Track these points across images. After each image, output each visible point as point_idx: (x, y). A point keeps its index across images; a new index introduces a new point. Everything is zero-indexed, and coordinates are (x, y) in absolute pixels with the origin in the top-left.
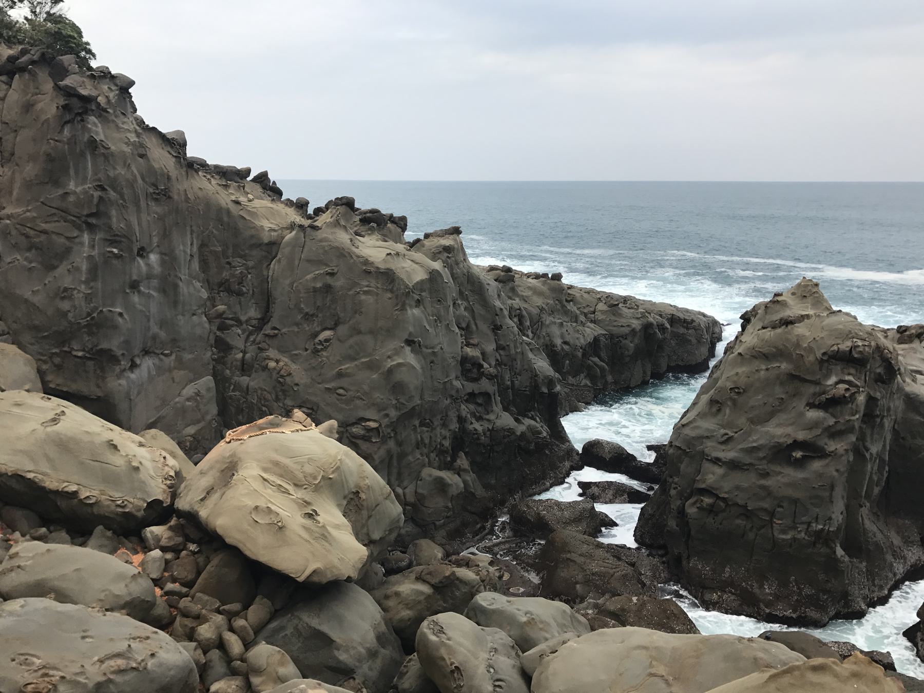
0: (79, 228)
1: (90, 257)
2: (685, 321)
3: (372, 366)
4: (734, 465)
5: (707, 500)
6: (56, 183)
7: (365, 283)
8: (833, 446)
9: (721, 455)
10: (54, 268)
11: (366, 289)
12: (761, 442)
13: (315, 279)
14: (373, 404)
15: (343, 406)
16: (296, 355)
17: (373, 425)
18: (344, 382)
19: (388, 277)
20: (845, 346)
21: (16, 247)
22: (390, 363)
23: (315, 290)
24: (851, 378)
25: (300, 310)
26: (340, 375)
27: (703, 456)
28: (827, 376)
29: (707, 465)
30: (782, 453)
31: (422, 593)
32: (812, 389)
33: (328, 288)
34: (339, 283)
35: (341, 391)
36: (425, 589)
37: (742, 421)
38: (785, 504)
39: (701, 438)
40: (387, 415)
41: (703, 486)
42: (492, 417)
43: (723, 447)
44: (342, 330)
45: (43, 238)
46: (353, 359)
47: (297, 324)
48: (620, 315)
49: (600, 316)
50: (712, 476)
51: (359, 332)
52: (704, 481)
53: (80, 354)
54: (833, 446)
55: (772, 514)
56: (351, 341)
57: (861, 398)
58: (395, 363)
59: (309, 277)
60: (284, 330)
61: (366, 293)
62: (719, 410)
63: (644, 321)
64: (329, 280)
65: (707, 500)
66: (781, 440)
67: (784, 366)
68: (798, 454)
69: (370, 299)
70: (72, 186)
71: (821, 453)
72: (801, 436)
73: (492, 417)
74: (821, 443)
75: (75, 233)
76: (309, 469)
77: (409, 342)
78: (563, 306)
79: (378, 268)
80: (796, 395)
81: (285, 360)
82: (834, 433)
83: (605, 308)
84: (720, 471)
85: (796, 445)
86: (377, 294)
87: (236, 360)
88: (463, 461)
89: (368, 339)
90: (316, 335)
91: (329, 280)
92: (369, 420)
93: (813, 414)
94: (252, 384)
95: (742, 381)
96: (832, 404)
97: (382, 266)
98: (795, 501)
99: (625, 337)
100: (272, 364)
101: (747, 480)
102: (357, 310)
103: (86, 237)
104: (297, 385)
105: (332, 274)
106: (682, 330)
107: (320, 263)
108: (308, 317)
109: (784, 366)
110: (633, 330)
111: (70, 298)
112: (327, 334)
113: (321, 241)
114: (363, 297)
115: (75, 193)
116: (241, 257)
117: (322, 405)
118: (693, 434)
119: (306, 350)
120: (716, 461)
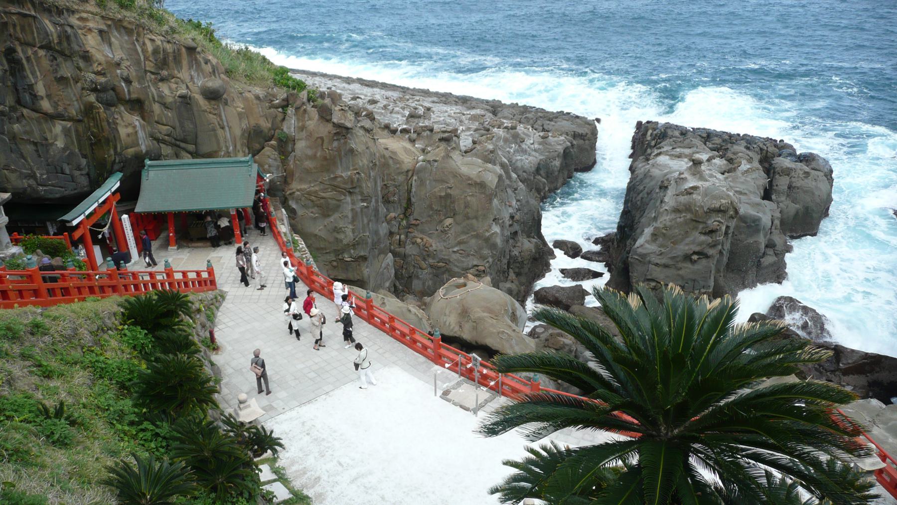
0: (345, 195)
1: (352, 210)
2: (582, 135)
3: (477, 236)
4: (666, 266)
5: (653, 284)
8: (711, 252)
9: (658, 262)
10: (329, 216)
12: (680, 253)
13: (440, 191)
19: (482, 185)
21: (305, 206)
22: (487, 234)
23: (441, 197)
24: (719, 219)
25: (432, 209)
28: (710, 218)
30: (687, 258)
32: (701, 226)
33: (448, 196)
34: (454, 192)
42: (519, 244)
44: (459, 218)
45: (322, 201)
47: (429, 216)
48: (550, 145)
51: (468, 218)
52: (651, 275)
53: (348, 259)
57: (724, 228)
59: (436, 190)
60: (423, 220)
62: (656, 239)
63: (565, 146)
64: (449, 191)
65: (653, 284)
67: (689, 216)
68: (695, 257)
70: (339, 172)
71: (707, 257)
72: (697, 249)
74: (705, 251)
75: (343, 197)
76: (498, 307)
80: (696, 228)
81: (426, 238)
82: (713, 246)
84: (658, 269)
85: (695, 253)
88: (512, 275)
89: (474, 221)
90: (441, 221)
91: (449, 191)
93: (703, 238)
95: (668, 224)
96: (712, 232)
98: (694, 280)
100: (419, 240)
102: (467, 206)
103: (349, 199)
105: (451, 188)
106: (581, 142)
107: (443, 181)
108: (438, 212)
109: (689, 216)
112: (449, 221)
114: (469, 198)
115: (342, 177)
116: (391, 180)
118: (644, 251)
120: (657, 265)
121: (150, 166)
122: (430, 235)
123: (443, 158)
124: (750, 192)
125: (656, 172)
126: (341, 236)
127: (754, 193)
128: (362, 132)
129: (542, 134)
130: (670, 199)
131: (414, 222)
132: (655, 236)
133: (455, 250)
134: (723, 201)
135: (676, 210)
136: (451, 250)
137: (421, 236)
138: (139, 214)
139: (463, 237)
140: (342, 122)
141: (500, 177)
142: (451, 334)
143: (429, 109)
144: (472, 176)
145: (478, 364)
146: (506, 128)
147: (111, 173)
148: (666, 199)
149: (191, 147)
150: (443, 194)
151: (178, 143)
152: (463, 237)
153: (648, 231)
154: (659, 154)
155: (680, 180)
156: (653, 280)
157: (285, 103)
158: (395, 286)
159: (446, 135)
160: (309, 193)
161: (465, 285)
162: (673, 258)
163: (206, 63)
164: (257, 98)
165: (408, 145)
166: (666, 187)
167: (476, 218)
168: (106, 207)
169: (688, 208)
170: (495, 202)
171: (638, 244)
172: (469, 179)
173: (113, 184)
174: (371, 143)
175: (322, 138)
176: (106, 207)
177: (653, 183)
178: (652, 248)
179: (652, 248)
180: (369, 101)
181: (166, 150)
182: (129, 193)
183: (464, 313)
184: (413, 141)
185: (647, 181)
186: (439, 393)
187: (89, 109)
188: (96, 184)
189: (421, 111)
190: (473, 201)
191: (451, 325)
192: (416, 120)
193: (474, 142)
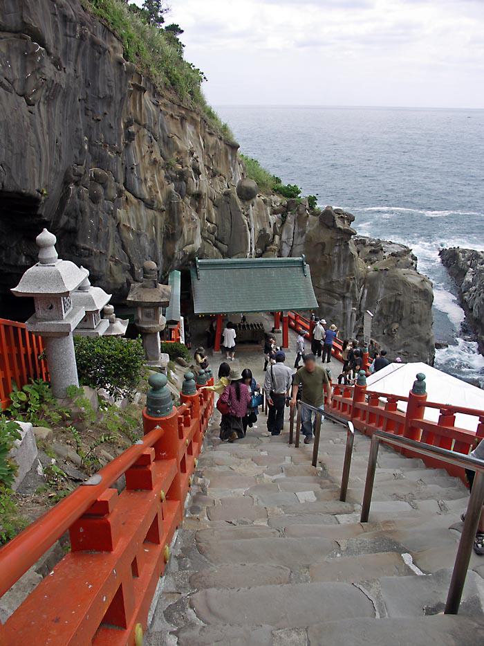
3: (420, 339)
6: (325, 276)
7: (414, 297)
22: (427, 337)
23: (390, 303)
26: (405, 345)
33: (398, 302)
35: (406, 354)
44: (405, 323)
51: (413, 323)
61: (417, 302)
69: (418, 305)
70: (334, 278)
75: (336, 301)
89: (417, 326)
97: (421, 288)
102: (413, 312)
113: (393, 277)
114: (415, 305)
119: (384, 334)
133: (401, 351)
136: (396, 352)
139: (408, 340)
144: (417, 285)
149: (225, 248)
150: (393, 300)
152: (408, 340)
167: (420, 323)
172: (416, 287)
175: (323, 244)
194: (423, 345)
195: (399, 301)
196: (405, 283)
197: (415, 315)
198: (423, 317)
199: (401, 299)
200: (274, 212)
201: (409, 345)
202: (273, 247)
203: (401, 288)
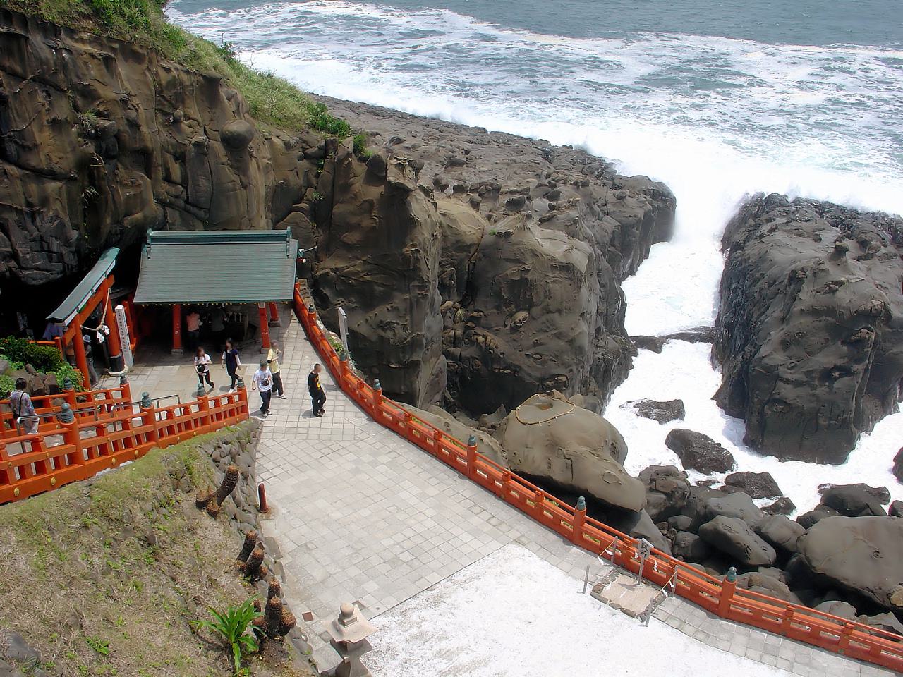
3: (559, 336)
4: (798, 384)
7: (552, 275)
8: (855, 367)
9: (789, 377)
11: (553, 279)
12: (816, 367)
14: (562, 364)
15: (540, 366)
16: (497, 330)
17: (564, 379)
18: (538, 349)
19: (568, 268)
20: (868, 306)
22: (572, 334)
26: (536, 345)
27: (778, 378)
29: (780, 384)
31: (661, 498)
36: (664, 497)
37: (803, 354)
38: (826, 405)
39: (776, 367)
40: (571, 370)
41: (777, 397)
42: (602, 343)
43: (789, 371)
44: (535, 311)
46: (542, 331)
49: (612, 209)
50: (786, 391)
51: (549, 312)
52: (779, 394)
54: (855, 367)
55: (818, 412)
56: (544, 319)
58: (577, 333)
66: (827, 366)
69: (557, 286)
72: (839, 362)
73: (602, 343)
77: (581, 316)
78: (592, 208)
79: (561, 263)
81: (490, 336)
83: (614, 200)
84: (789, 387)
85: (836, 368)
86: (561, 282)
87: (450, 337)
89: (556, 315)
90: (511, 315)
92: (559, 375)
94: (463, 353)
97: (564, 261)
99: (632, 226)
100: (481, 339)
101: (803, 391)
102: (548, 295)
104: (502, 353)
110: (639, 221)
111: (393, 330)
112: (522, 315)
113: (517, 244)
114: (551, 286)
117: (523, 366)
118: (772, 363)
119: (506, 326)
120: (787, 381)
121: (155, 239)
122: (496, 332)
123: (519, 229)
124: (892, 286)
125: (778, 255)
126: (389, 334)
127: (896, 287)
128: (421, 195)
129: (617, 192)
130: (807, 296)
131: (475, 314)
132: (785, 344)
134: (875, 303)
135: (814, 312)
137: (485, 333)
138: (139, 305)
140: (401, 181)
141: (590, 257)
142: (537, 473)
143: (467, 152)
144: (556, 256)
145: (648, 553)
146: (576, 184)
147: (107, 247)
148: (801, 295)
151: (188, 206)
153: (776, 335)
154: (772, 230)
155: (818, 272)
156: (782, 401)
157: (322, 152)
158: (445, 399)
159: (517, 196)
160: (347, 276)
161: (551, 406)
162: (807, 374)
163: (229, 99)
164: (288, 146)
165: (471, 211)
166: (801, 280)
167: (560, 311)
168: (100, 295)
169: (830, 311)
170: (584, 290)
171: (764, 351)
172: (553, 259)
173: (107, 263)
174: (432, 208)
176: (100, 295)
177: (774, 270)
178: (779, 358)
179: (779, 358)
180: (392, 140)
181: (173, 215)
182: (126, 276)
183: (554, 445)
184: (475, 205)
185: (766, 265)
186: (589, 589)
187: (85, 165)
188: (87, 263)
189: (461, 157)
190: (555, 288)
191: (537, 461)
192: (459, 169)
193: (552, 208)
194: (563, 343)
195: (527, 279)
196: (535, 254)
197: (552, 300)
198: (565, 304)
199: (529, 276)
200: (306, 157)
201: (541, 344)
202: (303, 205)
203: (530, 260)
